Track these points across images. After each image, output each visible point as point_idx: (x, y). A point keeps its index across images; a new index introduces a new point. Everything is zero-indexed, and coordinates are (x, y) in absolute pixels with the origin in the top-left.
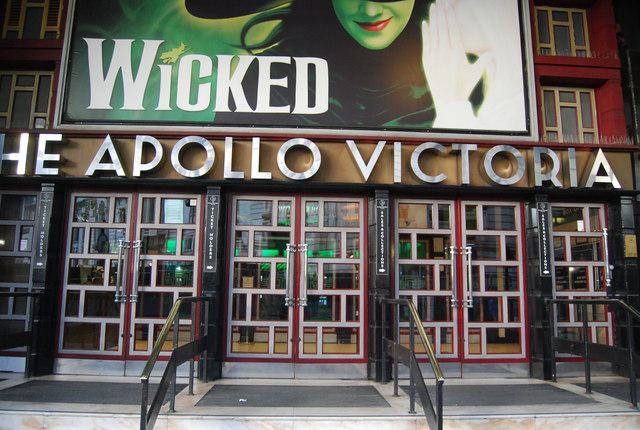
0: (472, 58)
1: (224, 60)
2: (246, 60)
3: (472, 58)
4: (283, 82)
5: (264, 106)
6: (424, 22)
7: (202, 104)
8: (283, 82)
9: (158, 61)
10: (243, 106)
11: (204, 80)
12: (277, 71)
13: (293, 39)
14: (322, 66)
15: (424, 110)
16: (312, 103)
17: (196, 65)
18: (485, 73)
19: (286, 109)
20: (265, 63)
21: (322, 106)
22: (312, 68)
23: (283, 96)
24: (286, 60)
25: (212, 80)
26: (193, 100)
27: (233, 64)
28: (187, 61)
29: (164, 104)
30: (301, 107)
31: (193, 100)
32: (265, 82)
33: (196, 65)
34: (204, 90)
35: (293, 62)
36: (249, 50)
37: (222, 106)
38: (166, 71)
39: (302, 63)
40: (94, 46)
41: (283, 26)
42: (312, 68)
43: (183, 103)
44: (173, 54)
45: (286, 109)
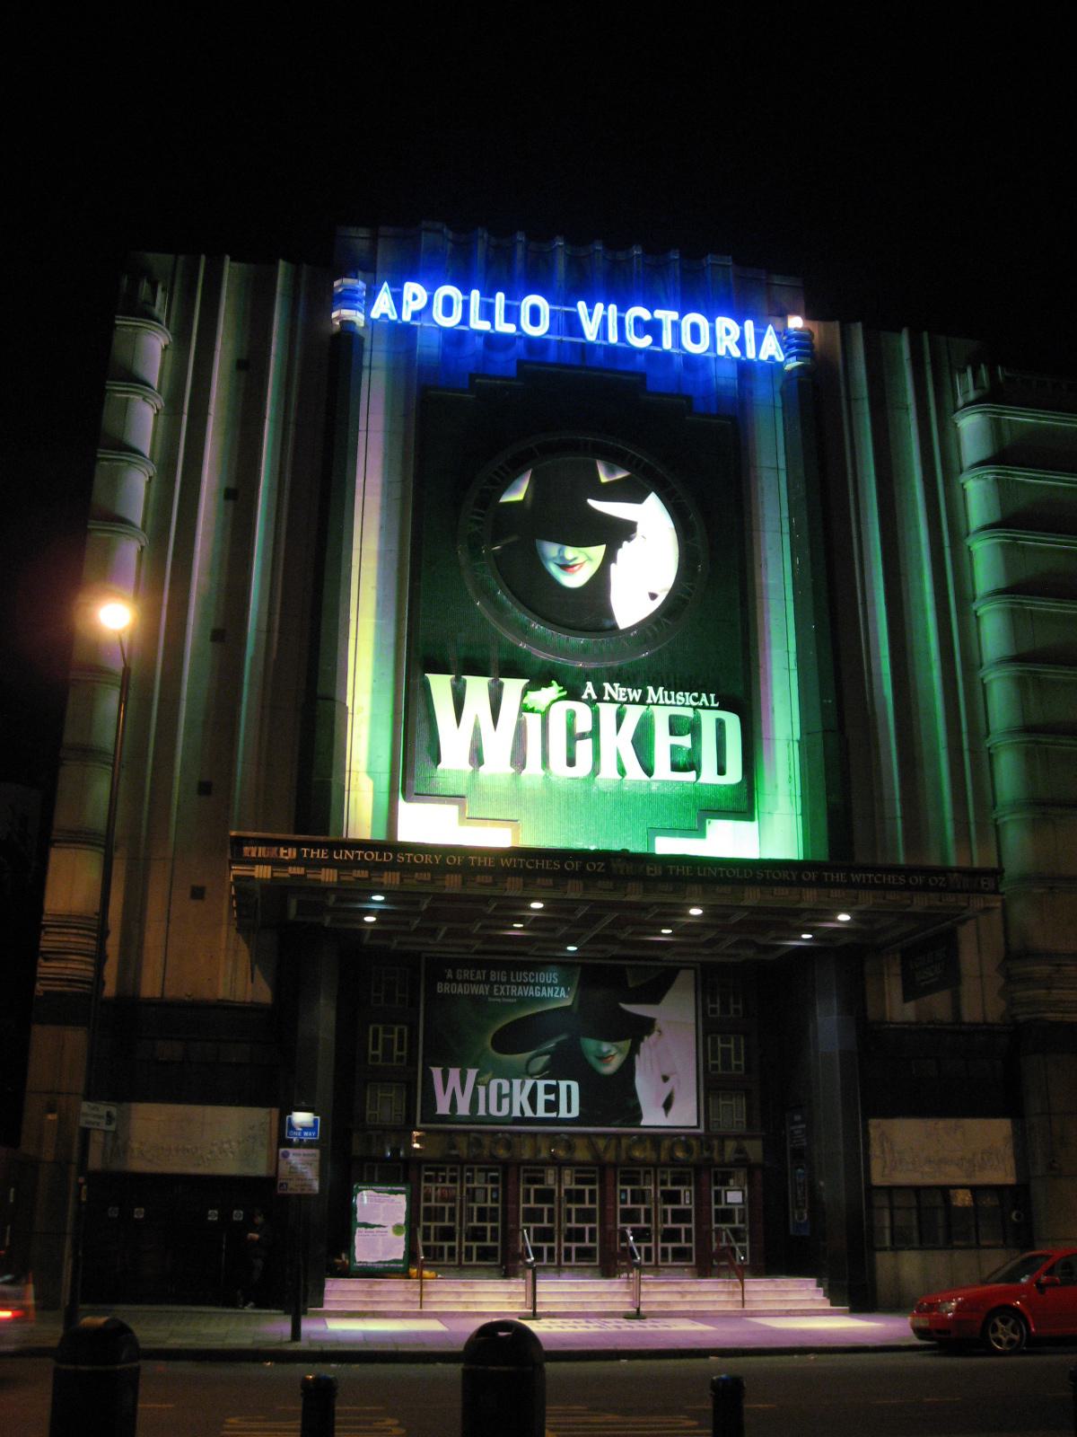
0: (665, 1079)
1: (517, 1082)
2: (529, 1083)
3: (665, 1079)
4: (552, 1097)
5: (541, 1113)
6: (637, 1056)
7: (505, 1112)
8: (552, 1097)
9: (477, 1083)
10: (529, 1113)
11: (505, 1096)
12: (549, 1089)
13: (557, 1070)
14: (575, 1086)
15: (635, 1114)
16: (569, 1110)
17: (500, 1086)
18: (673, 1087)
19: (554, 1115)
20: (541, 1084)
21: (575, 1113)
22: (569, 1087)
23: (552, 1106)
24: (553, 1082)
25: (510, 1095)
26: (499, 1109)
27: (522, 1085)
28: (494, 1084)
29: (482, 1112)
30: (563, 1113)
31: (499, 1109)
32: (542, 1097)
33: (500, 1086)
34: (505, 1102)
35: (558, 1084)
36: (531, 1076)
37: (516, 1113)
38: (482, 1089)
39: (563, 1084)
40: (437, 1072)
41: (550, 1060)
42: (569, 1087)
43: (493, 1111)
44: (485, 1078)
45: (554, 1115)
